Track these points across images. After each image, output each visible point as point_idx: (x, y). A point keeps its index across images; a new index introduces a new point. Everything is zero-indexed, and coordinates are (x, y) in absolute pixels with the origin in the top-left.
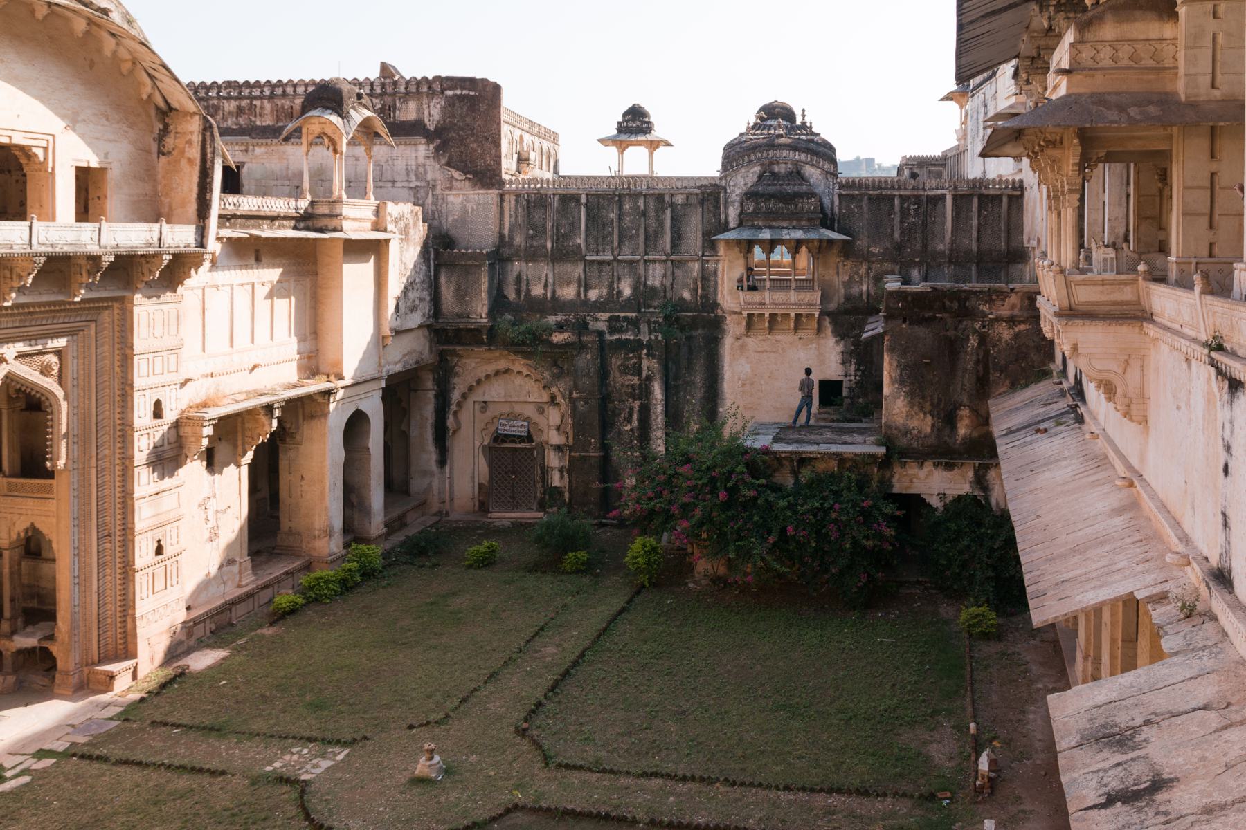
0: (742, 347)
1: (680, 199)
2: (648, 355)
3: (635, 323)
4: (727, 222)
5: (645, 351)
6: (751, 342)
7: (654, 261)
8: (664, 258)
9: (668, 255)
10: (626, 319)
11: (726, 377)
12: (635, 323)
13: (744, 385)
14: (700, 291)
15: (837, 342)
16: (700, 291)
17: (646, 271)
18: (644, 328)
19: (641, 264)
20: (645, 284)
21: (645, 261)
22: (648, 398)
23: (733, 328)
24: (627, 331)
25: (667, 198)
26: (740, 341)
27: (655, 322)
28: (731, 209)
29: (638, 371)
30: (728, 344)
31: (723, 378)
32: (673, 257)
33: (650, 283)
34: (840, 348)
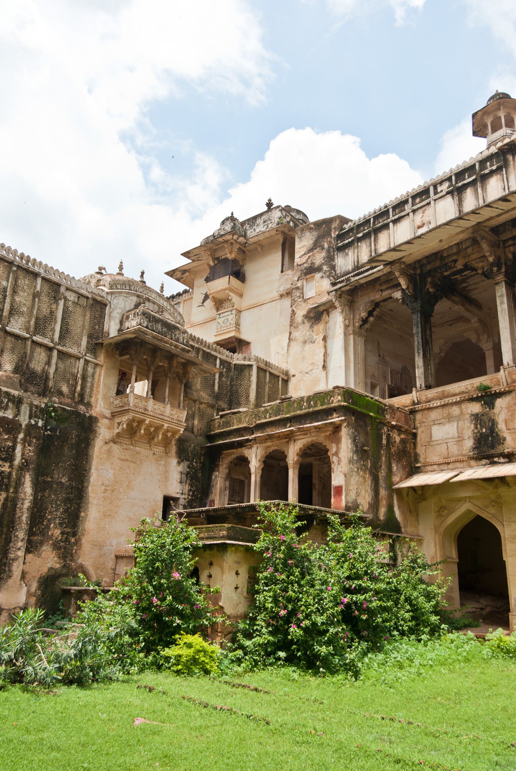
0: (109, 451)
1: (72, 297)
2: (24, 440)
3: (18, 402)
4: (109, 334)
5: (21, 436)
6: (116, 449)
7: (40, 345)
8: (51, 345)
9: (56, 344)
10: (7, 394)
11: (92, 479)
12: (18, 402)
13: (106, 490)
14: (79, 388)
15: (179, 463)
16: (79, 388)
17: (32, 352)
18: (25, 409)
19: (29, 343)
20: (28, 365)
21: (33, 342)
22: (16, 491)
23: (104, 432)
24: (6, 408)
25: (62, 289)
26: (106, 447)
27: (37, 407)
28: (112, 323)
29: (10, 458)
30: (98, 448)
31: (88, 481)
32: (59, 347)
33: (32, 366)
34: (180, 468)
